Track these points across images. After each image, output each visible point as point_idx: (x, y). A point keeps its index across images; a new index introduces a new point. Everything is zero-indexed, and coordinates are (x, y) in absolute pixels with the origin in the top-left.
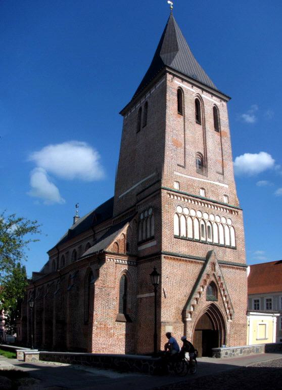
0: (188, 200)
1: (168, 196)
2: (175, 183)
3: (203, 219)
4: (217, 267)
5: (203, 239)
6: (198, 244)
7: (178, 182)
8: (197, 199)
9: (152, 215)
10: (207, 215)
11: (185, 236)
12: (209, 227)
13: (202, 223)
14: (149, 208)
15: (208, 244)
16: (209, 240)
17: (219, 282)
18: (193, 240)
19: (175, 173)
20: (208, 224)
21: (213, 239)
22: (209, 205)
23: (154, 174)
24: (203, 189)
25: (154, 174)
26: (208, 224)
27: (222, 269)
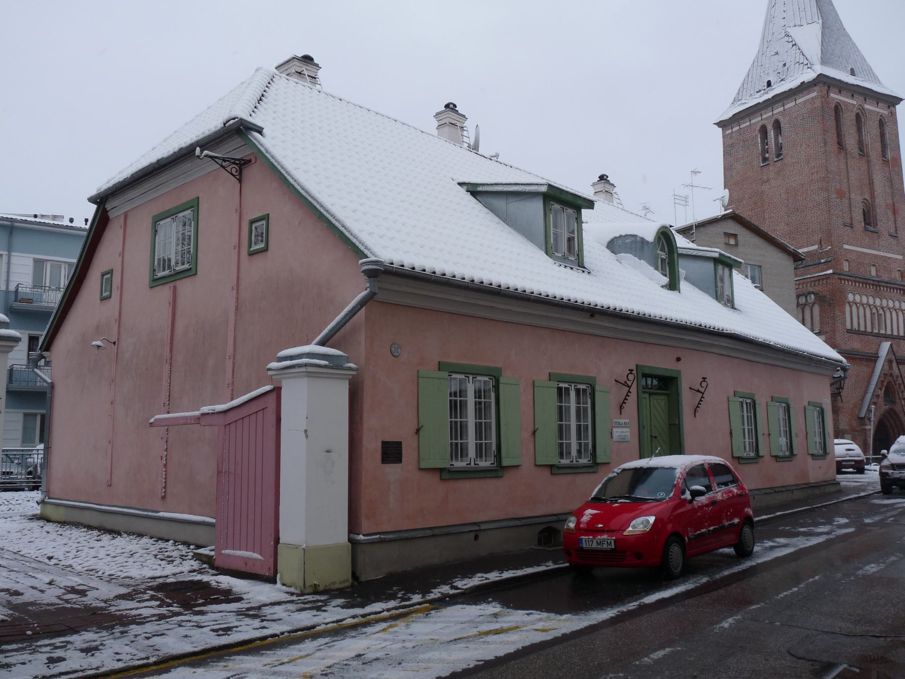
0: (859, 283)
1: (839, 281)
2: (844, 262)
3: (875, 306)
4: (894, 364)
5: (876, 331)
6: (870, 337)
7: (848, 261)
8: (869, 282)
9: (814, 304)
10: (880, 300)
11: (857, 329)
12: (881, 314)
13: (874, 311)
14: (809, 293)
15: (880, 337)
16: (883, 332)
17: (897, 383)
18: (865, 333)
19: (846, 247)
20: (881, 312)
21: (886, 330)
22: (882, 288)
23: (815, 247)
24: (874, 265)
25: (815, 247)
26: (881, 312)
27: (900, 367)
